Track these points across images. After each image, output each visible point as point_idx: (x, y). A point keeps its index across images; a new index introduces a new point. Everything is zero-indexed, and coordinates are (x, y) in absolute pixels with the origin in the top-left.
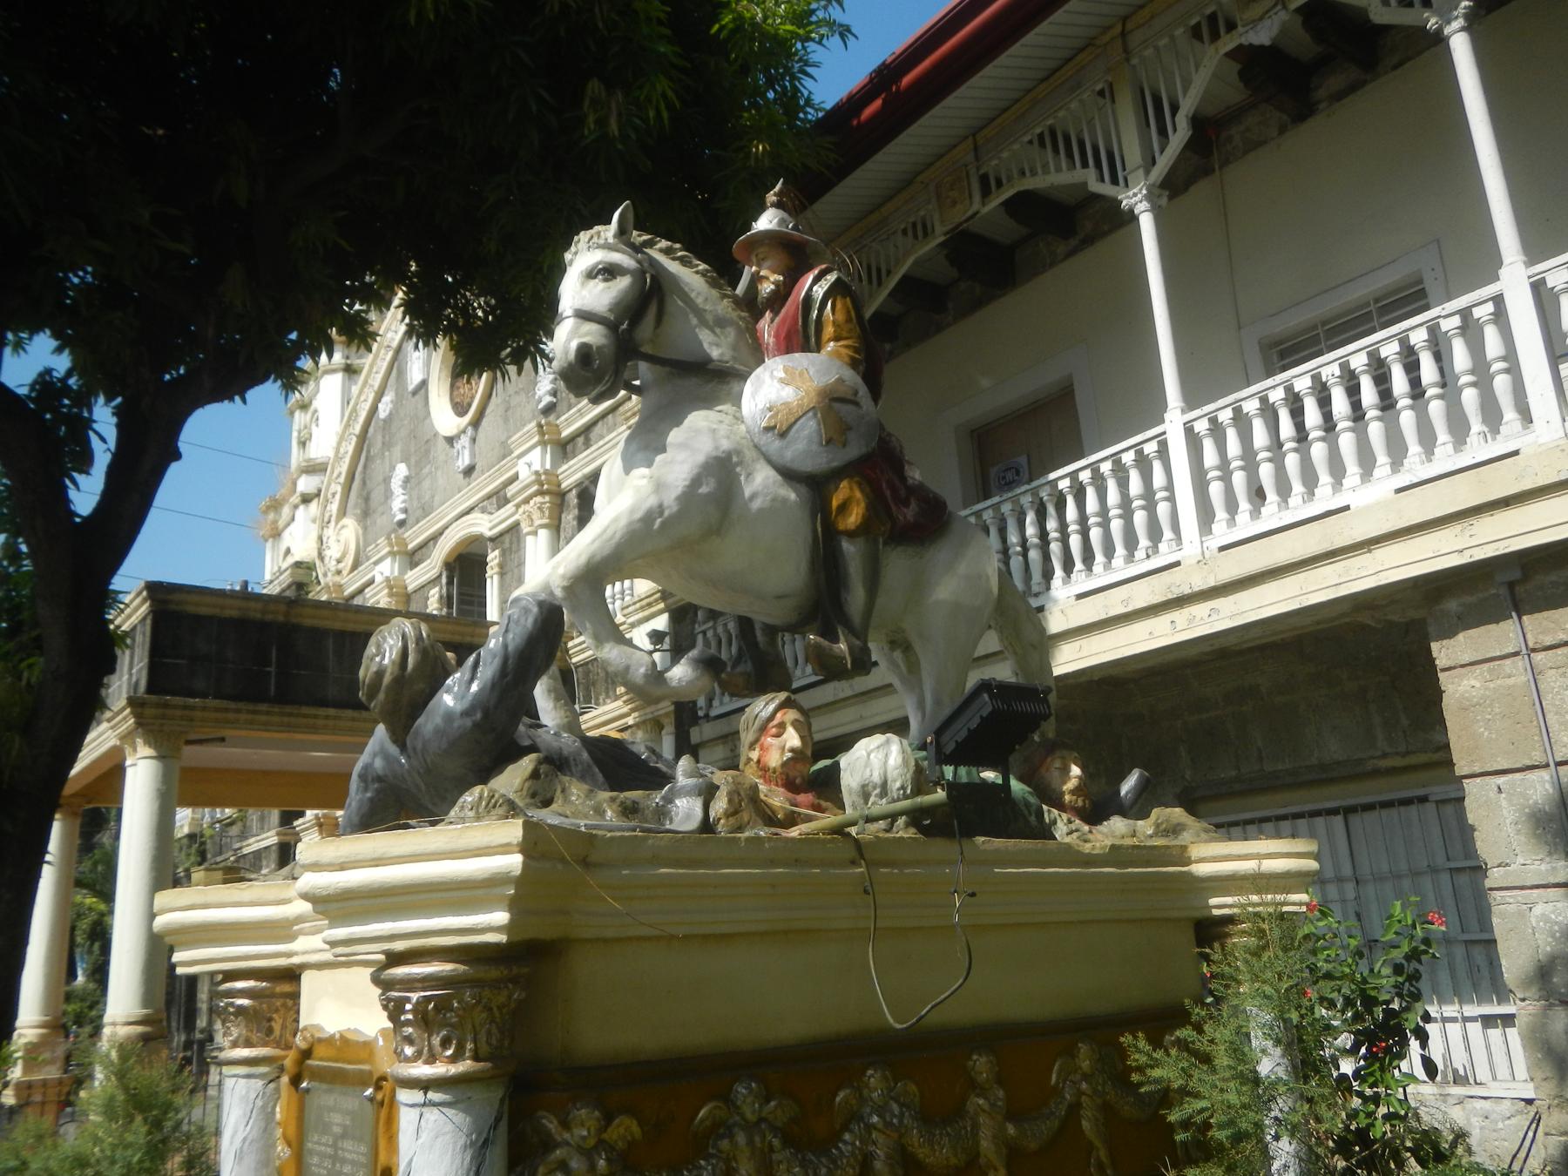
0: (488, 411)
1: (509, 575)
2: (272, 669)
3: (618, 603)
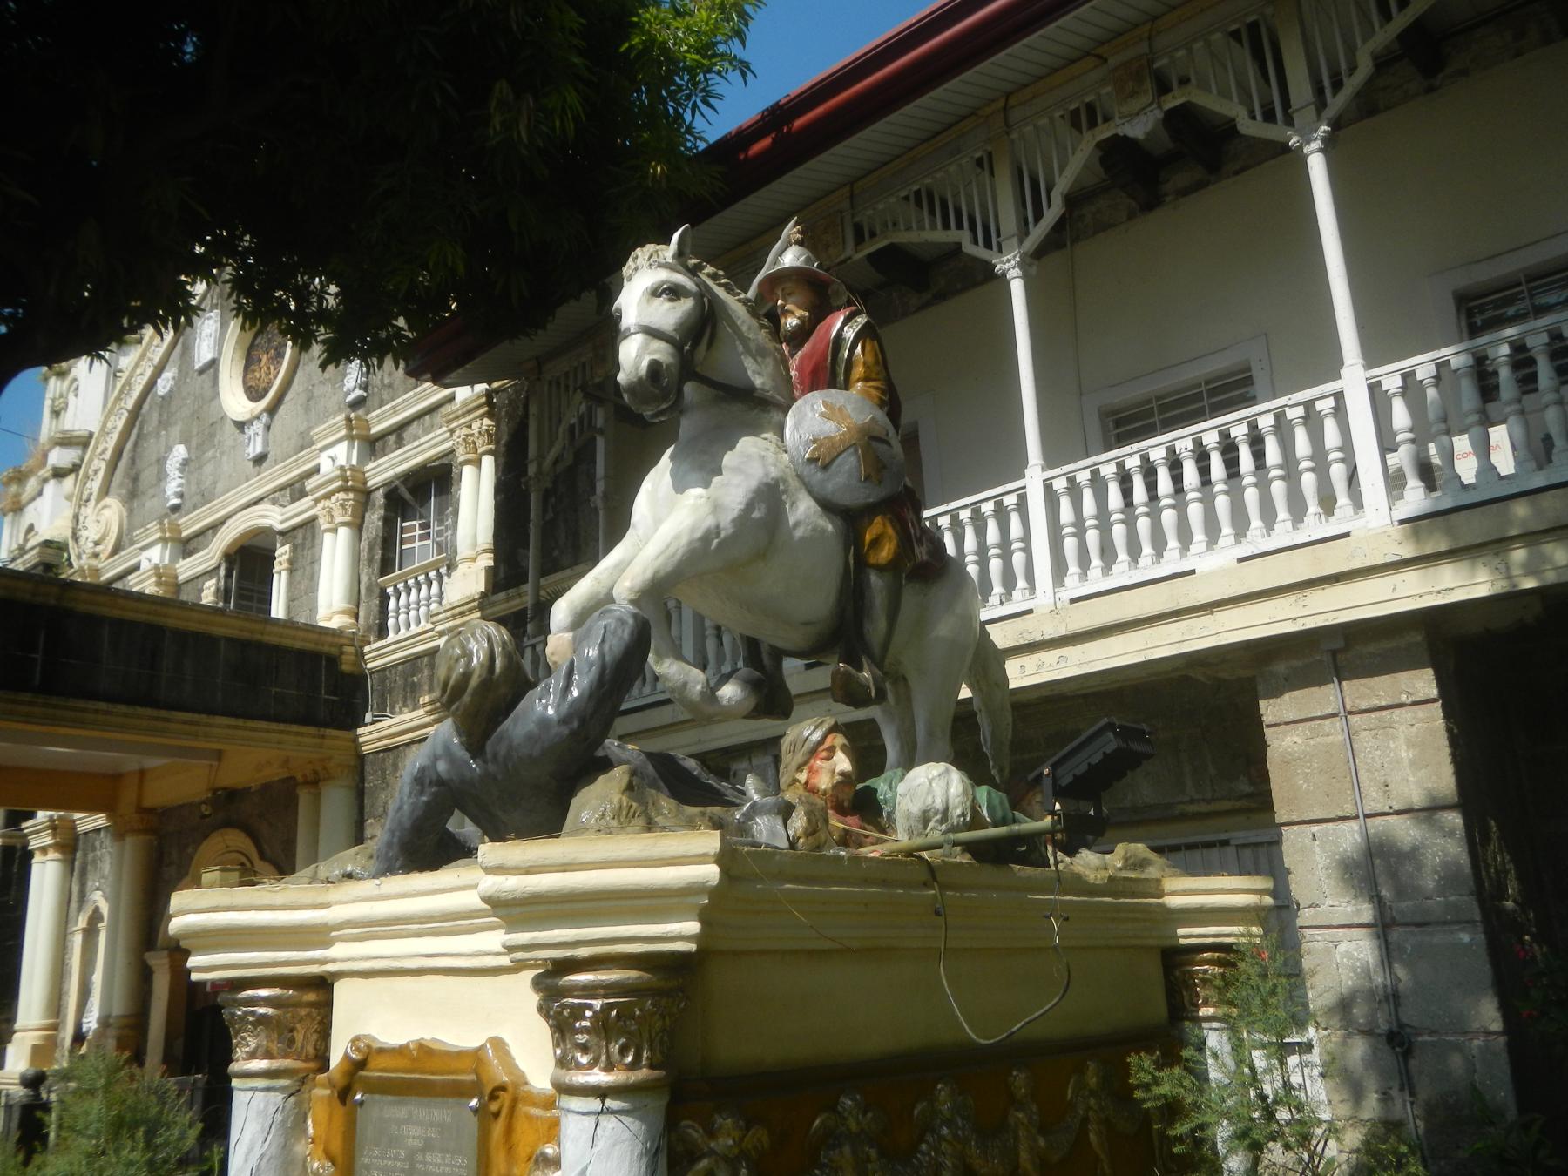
0: (287, 398)
1: (299, 573)
2: (38, 656)
3: (423, 610)
